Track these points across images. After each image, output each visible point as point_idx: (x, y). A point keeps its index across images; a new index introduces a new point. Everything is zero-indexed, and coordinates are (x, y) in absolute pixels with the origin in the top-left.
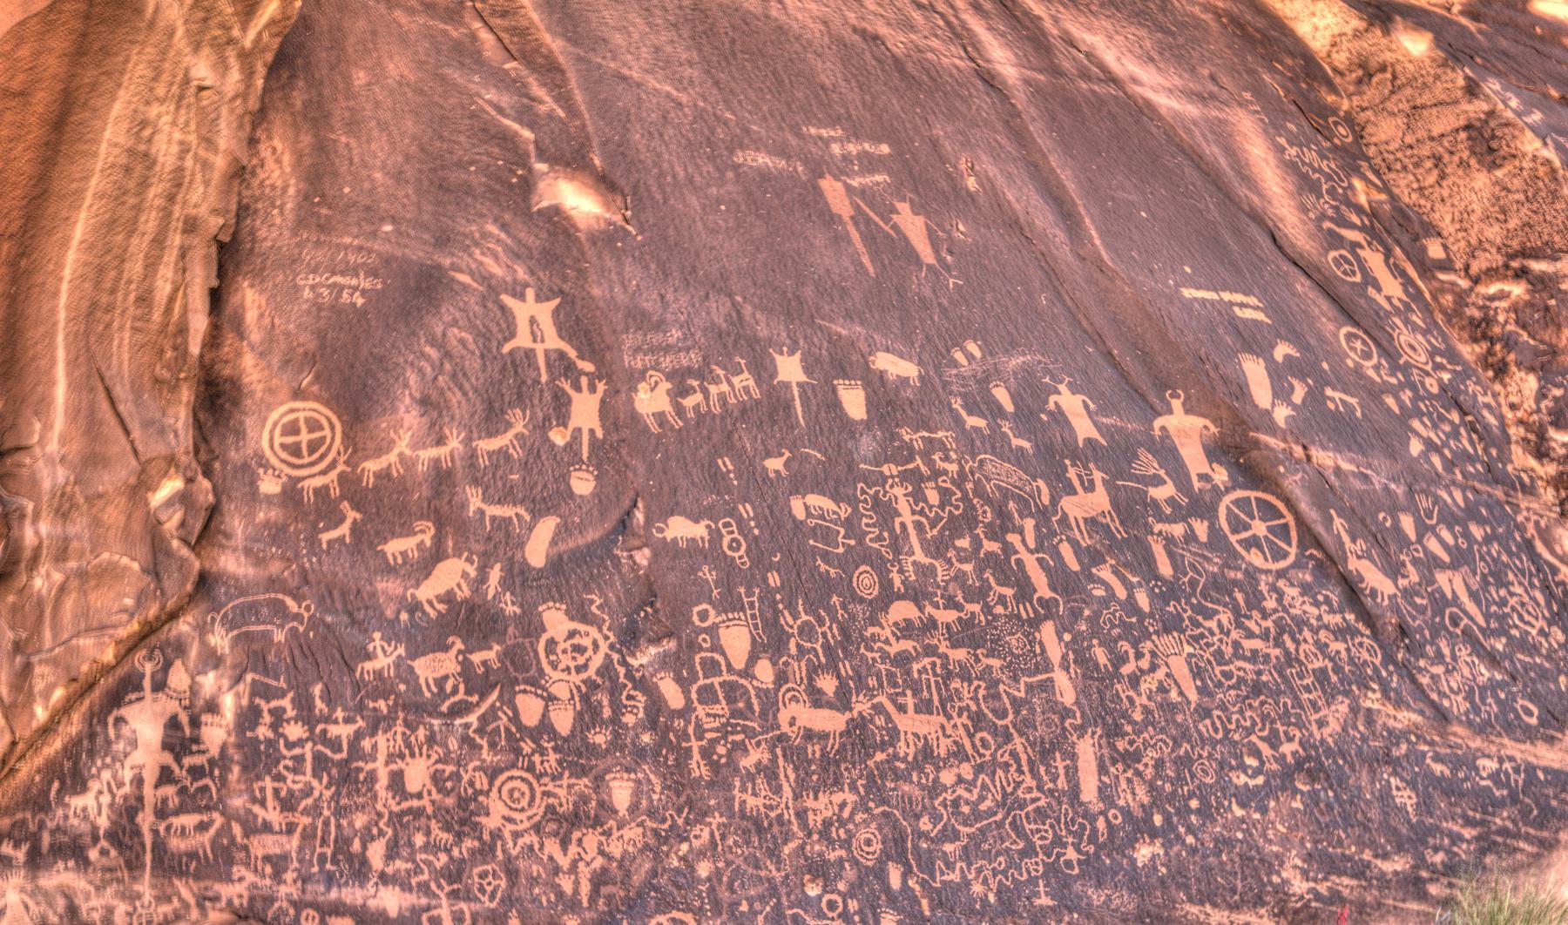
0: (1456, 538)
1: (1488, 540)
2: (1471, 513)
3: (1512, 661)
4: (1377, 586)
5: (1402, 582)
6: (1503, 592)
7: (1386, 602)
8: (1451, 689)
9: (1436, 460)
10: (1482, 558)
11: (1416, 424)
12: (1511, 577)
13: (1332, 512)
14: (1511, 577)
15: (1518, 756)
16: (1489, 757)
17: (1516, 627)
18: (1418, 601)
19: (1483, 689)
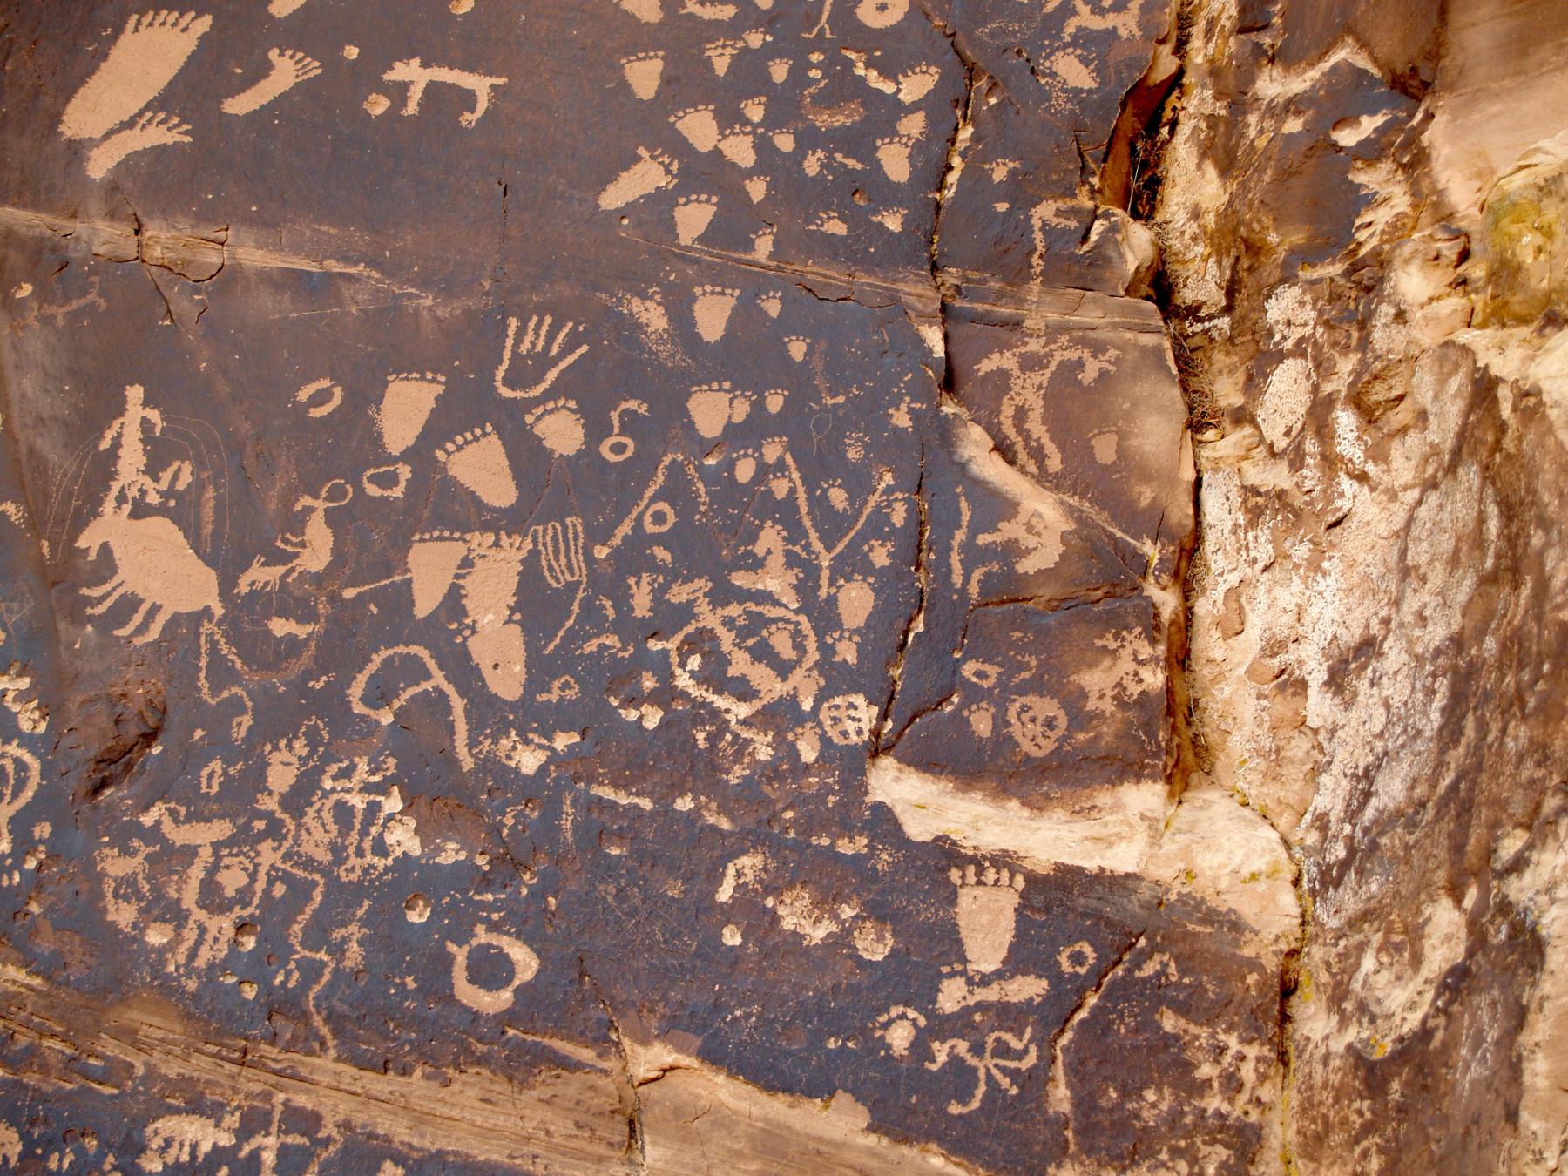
0: (596, 429)
1: (739, 436)
2: (744, 359)
3: (552, 810)
4: (151, 591)
5: (260, 575)
6: (679, 594)
7: (154, 632)
8: (211, 896)
9: (694, 218)
10: (676, 491)
11: (699, 127)
12: (770, 539)
13: (135, 393)
14: (770, 539)
15: (334, 1110)
16: (215, 1112)
17: (666, 695)
18: (280, 627)
19: (343, 896)
